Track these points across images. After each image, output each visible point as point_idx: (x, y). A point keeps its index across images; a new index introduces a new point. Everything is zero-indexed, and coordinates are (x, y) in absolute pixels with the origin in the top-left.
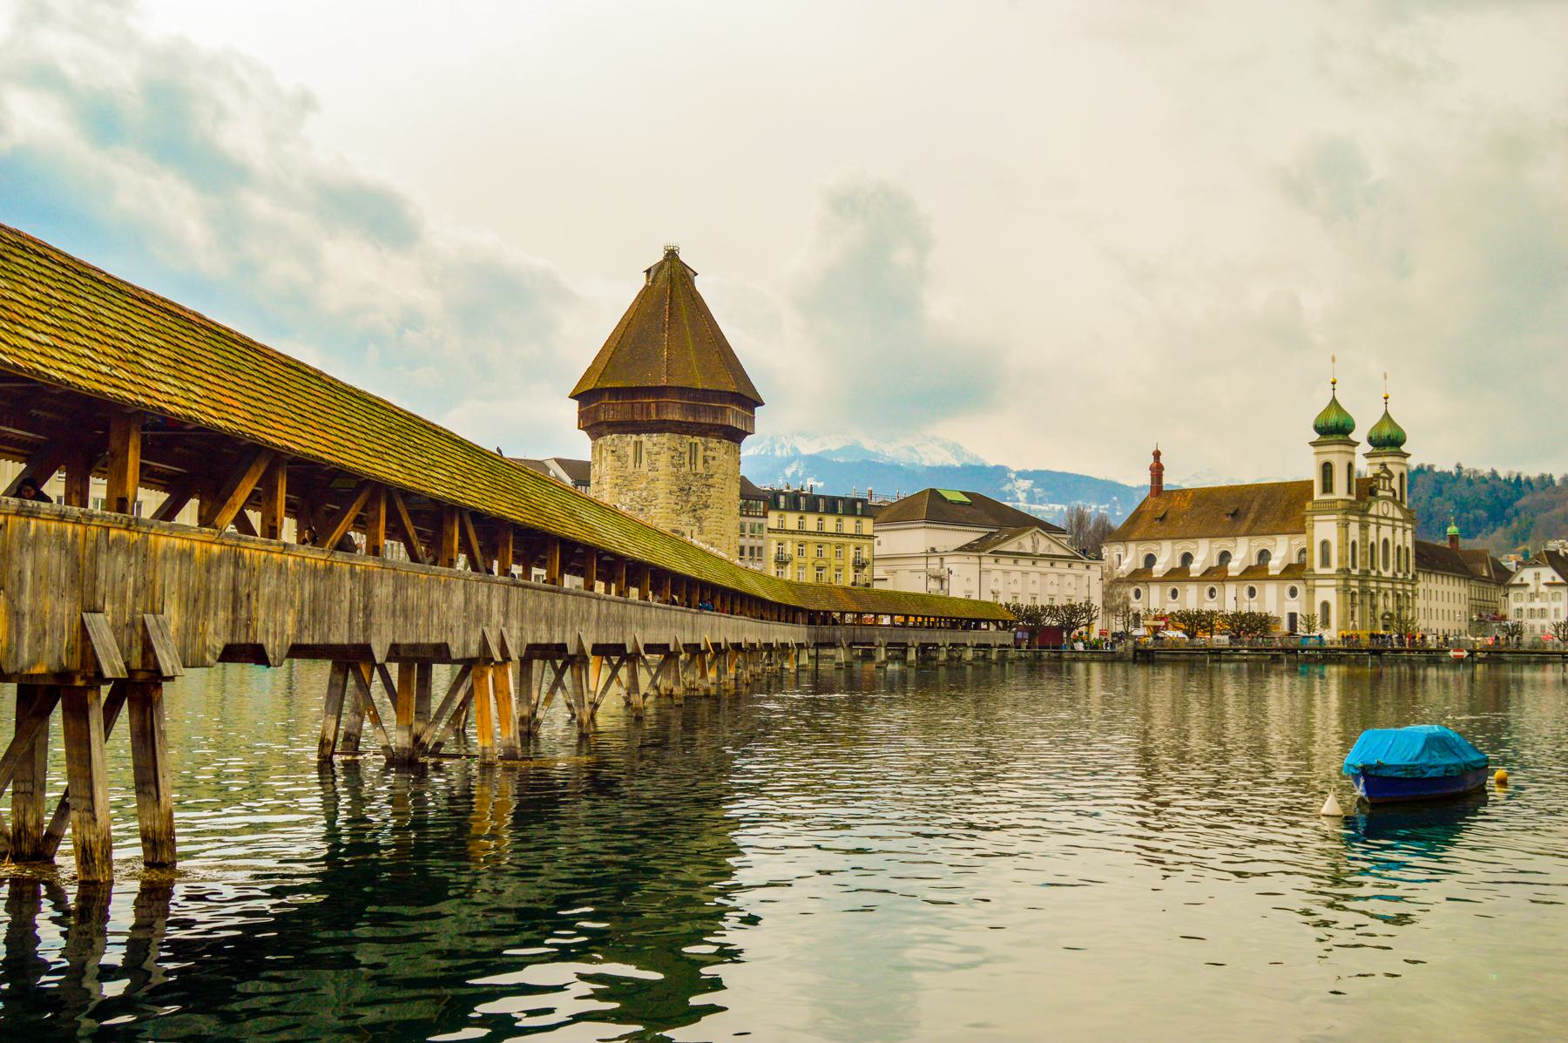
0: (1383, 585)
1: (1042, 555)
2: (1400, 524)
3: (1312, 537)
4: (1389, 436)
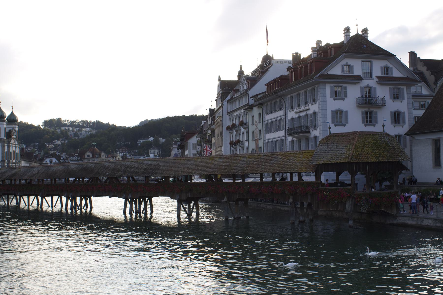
2: (17, 146)
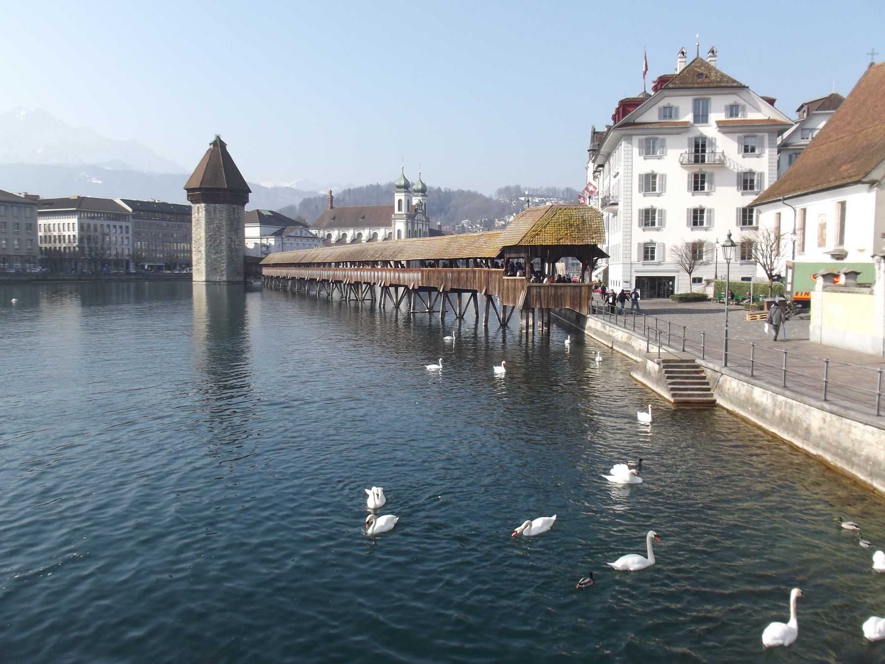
2: (424, 223)
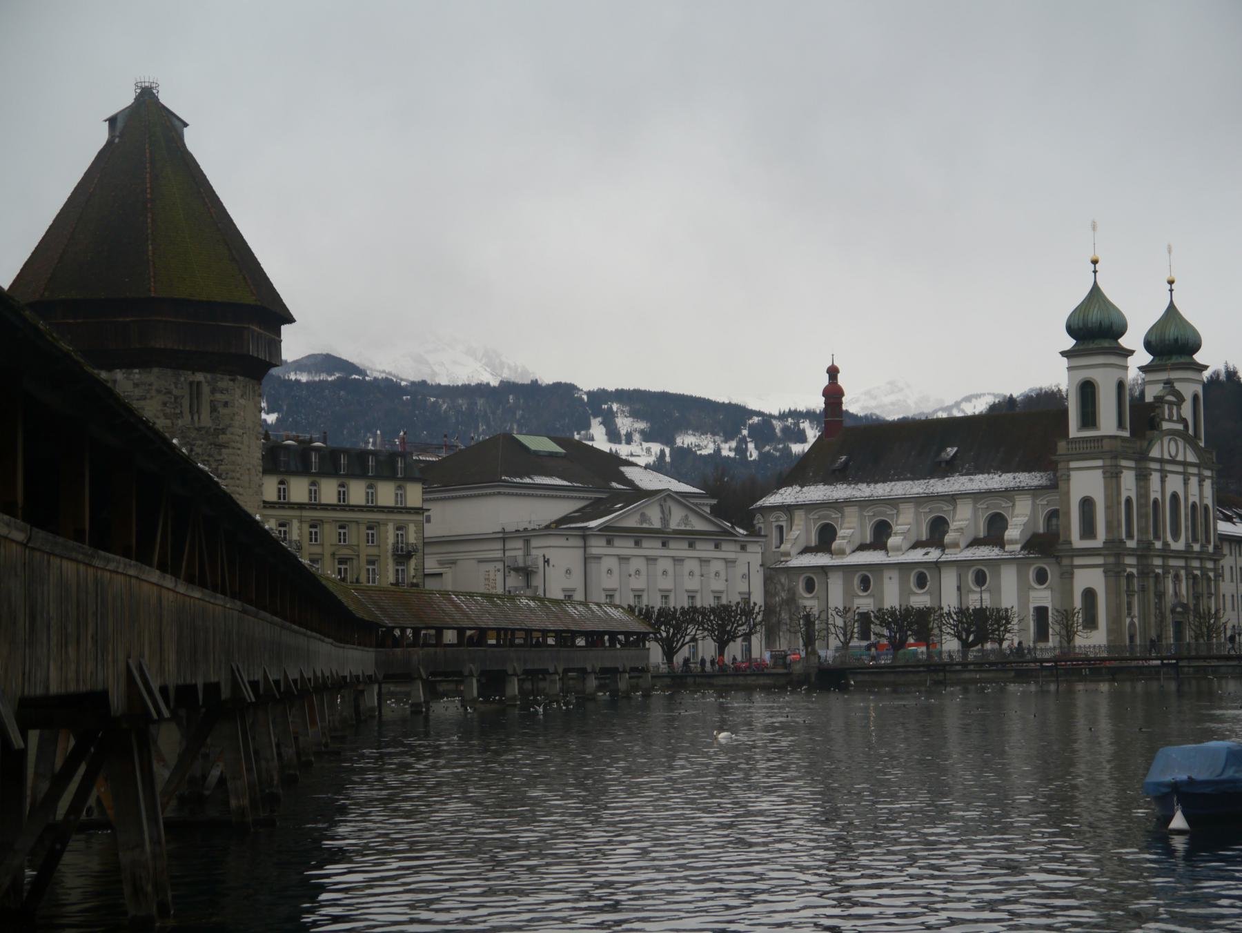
0: (1172, 562)
1: (676, 532)
3: (1068, 493)
4: (1176, 340)
